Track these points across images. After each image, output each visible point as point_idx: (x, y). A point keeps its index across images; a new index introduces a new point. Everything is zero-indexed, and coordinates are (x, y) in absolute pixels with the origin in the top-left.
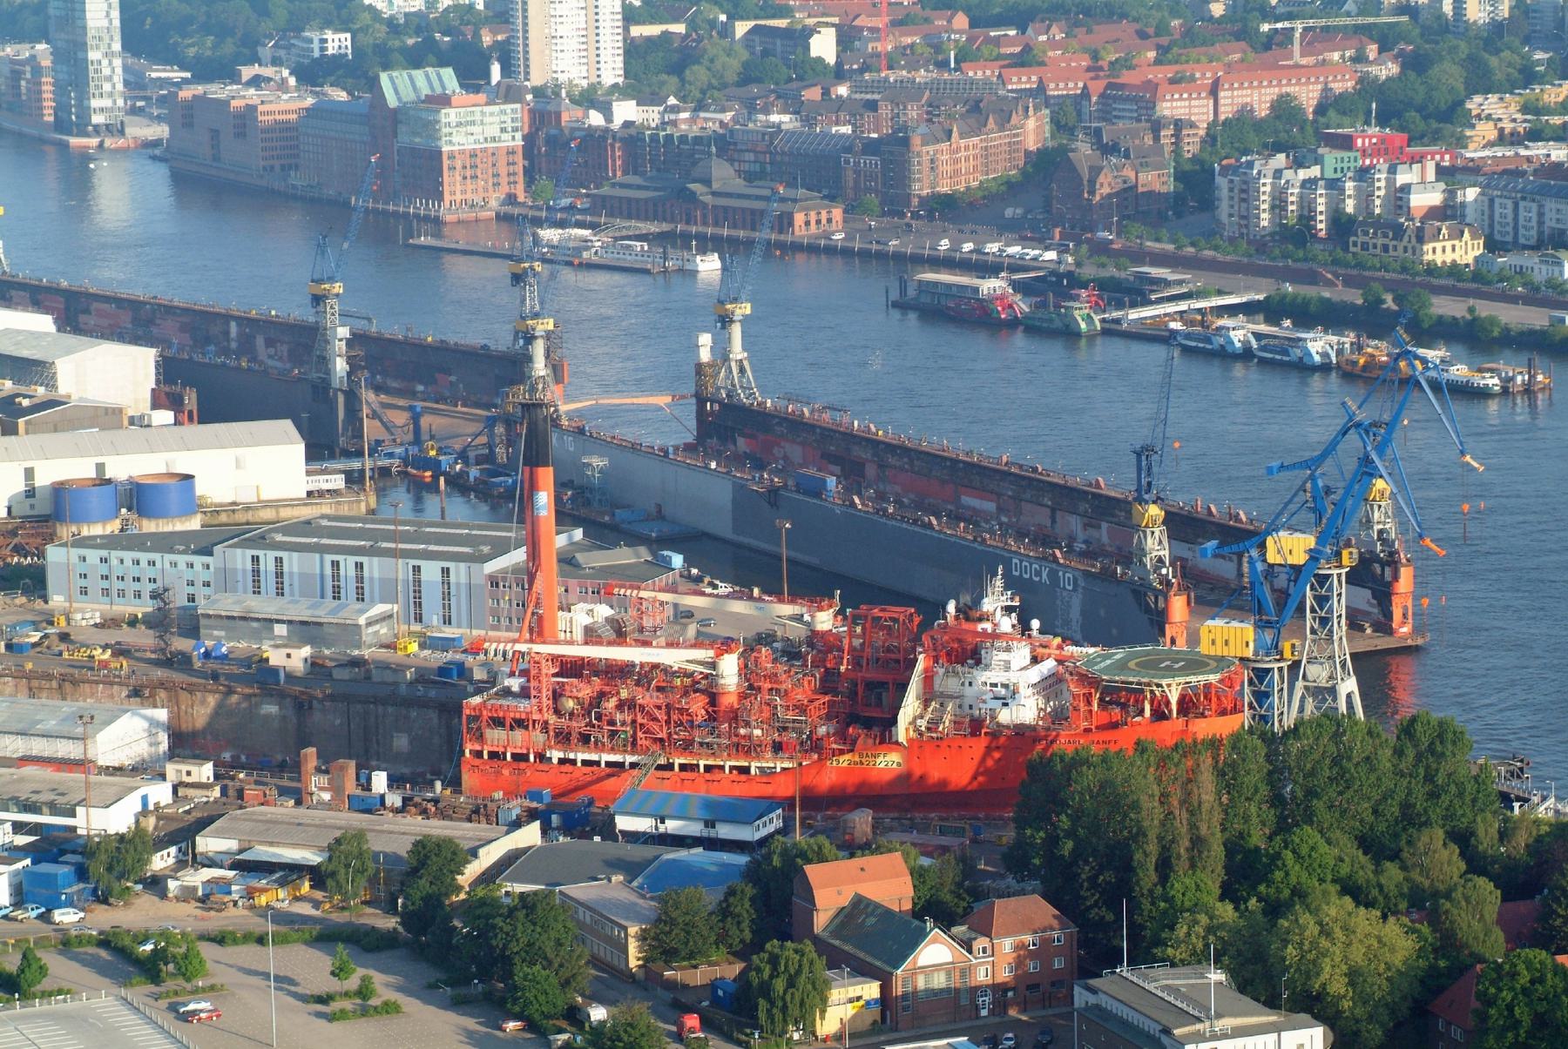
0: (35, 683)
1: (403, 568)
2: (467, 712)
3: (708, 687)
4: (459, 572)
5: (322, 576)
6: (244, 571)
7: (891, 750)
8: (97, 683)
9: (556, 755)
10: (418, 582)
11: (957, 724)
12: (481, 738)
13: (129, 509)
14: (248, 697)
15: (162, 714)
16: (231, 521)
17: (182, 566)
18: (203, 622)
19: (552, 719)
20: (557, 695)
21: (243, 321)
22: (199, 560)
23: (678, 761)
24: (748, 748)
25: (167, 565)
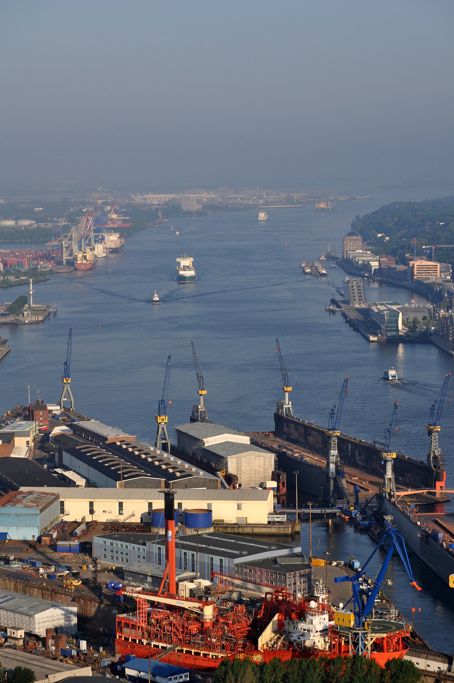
0: (44, 592)
1: (206, 557)
2: (117, 620)
3: (199, 618)
4: (226, 561)
5: (181, 558)
6: (156, 553)
7: (258, 653)
8: (62, 594)
9: (145, 642)
10: (212, 564)
11: (284, 645)
12: (121, 631)
13: (182, 523)
14: (107, 605)
15: (75, 609)
16: (233, 531)
17: (136, 549)
18: (125, 573)
19: (144, 625)
20: (149, 614)
21: (354, 444)
22: (141, 547)
23: (185, 649)
24: (210, 647)
25: (131, 548)
